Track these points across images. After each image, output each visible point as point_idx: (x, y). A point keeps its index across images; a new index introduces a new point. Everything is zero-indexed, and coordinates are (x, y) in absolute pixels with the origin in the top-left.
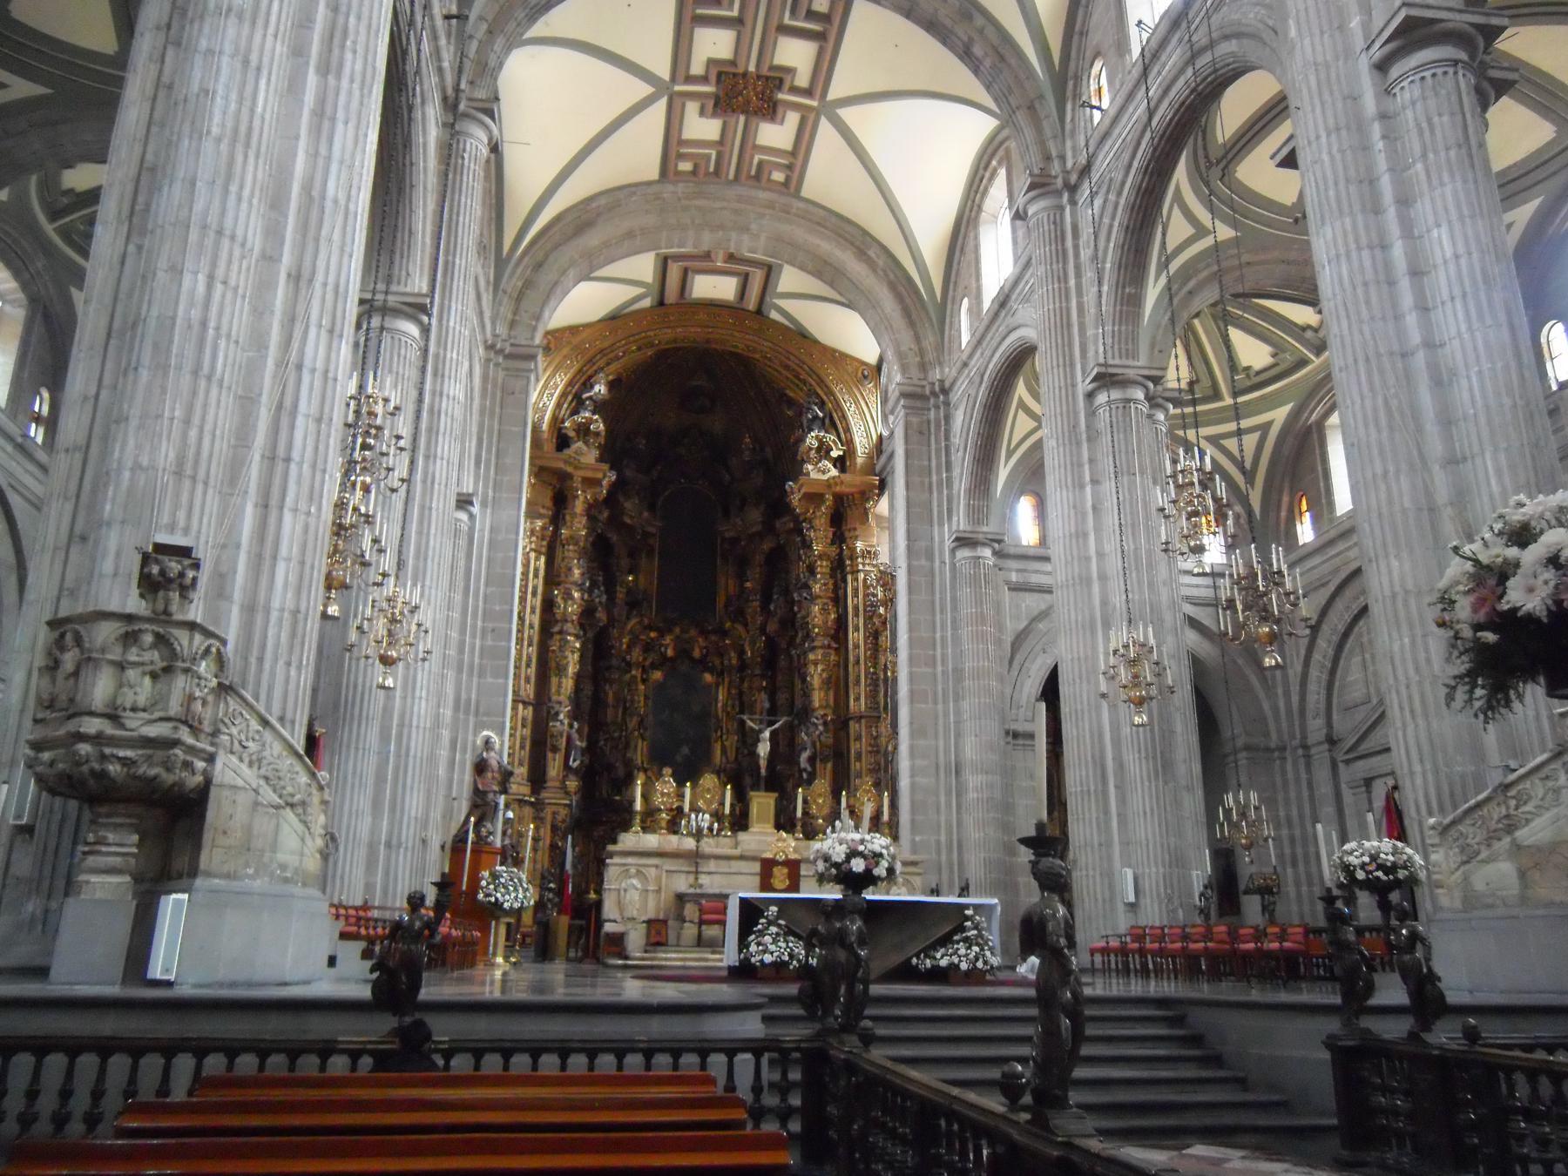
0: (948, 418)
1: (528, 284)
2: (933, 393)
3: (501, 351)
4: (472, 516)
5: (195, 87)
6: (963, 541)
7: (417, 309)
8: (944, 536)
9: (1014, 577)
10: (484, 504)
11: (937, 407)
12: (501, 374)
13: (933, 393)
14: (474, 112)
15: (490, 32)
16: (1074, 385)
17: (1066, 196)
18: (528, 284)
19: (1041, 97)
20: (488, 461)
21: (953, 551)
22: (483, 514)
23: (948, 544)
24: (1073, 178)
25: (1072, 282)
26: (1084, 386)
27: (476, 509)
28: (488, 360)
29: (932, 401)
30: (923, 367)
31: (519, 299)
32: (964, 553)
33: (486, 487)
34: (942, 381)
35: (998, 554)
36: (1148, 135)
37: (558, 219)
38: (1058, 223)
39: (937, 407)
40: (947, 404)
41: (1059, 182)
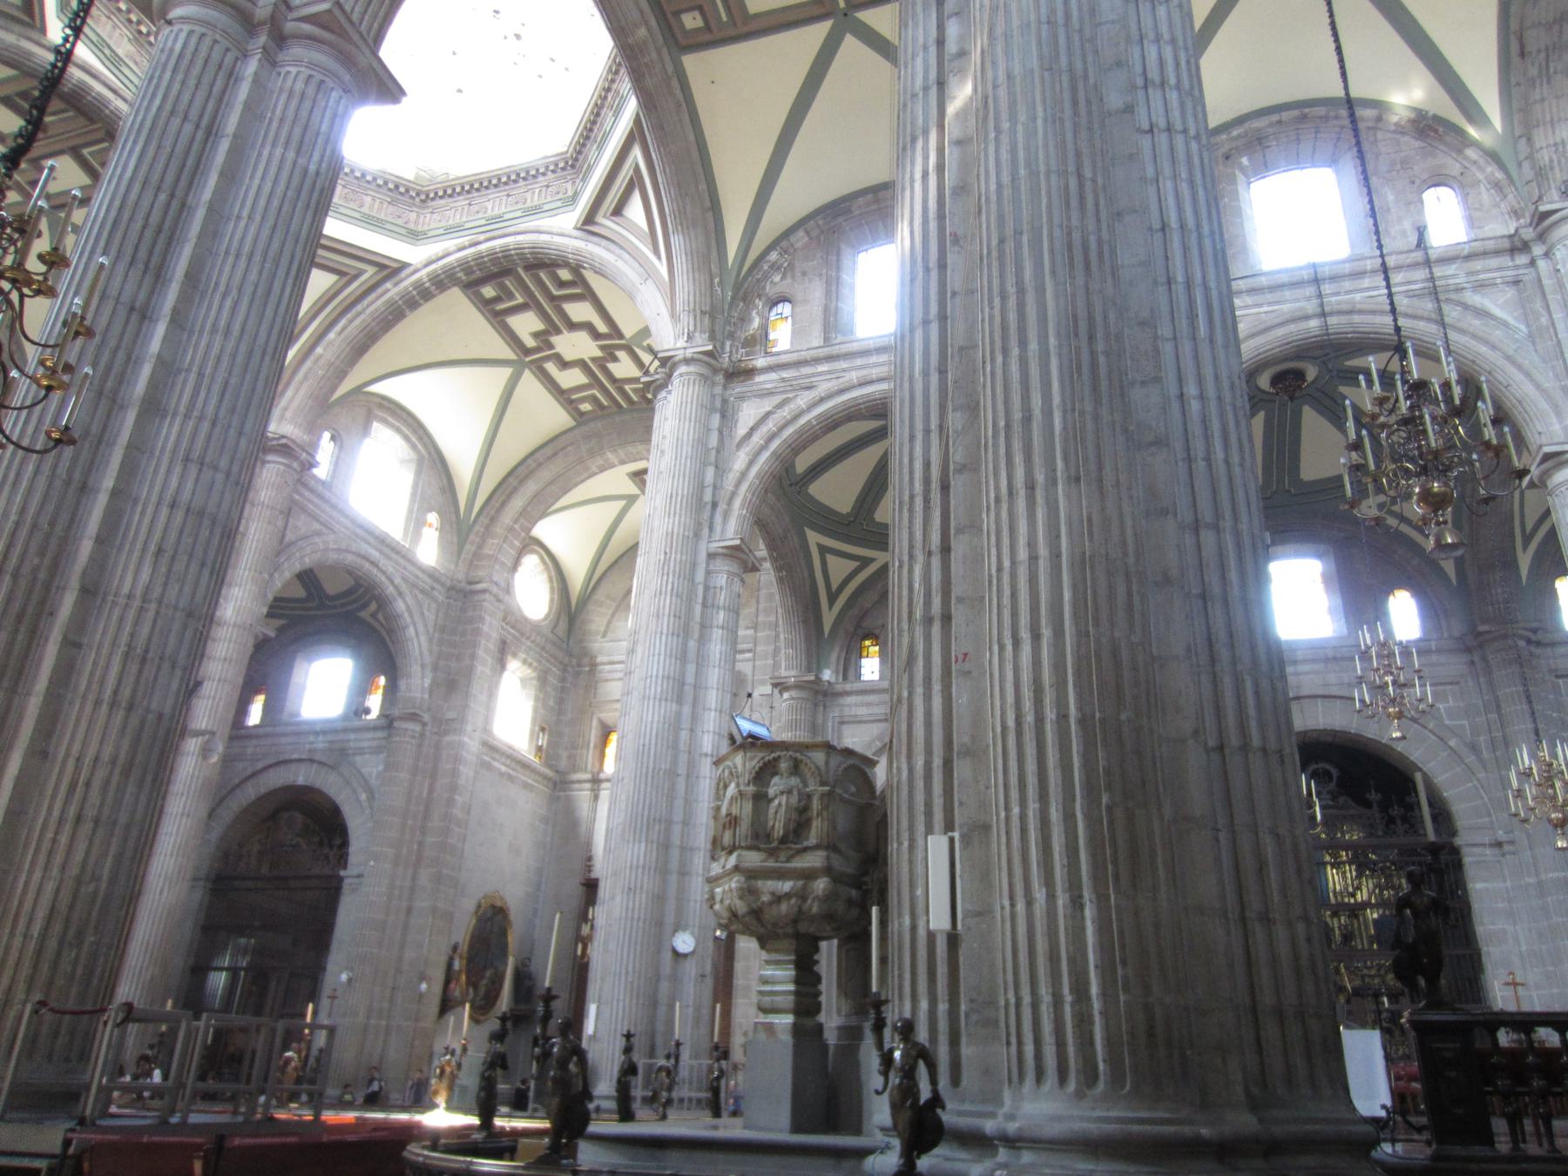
14: (1540, 228)
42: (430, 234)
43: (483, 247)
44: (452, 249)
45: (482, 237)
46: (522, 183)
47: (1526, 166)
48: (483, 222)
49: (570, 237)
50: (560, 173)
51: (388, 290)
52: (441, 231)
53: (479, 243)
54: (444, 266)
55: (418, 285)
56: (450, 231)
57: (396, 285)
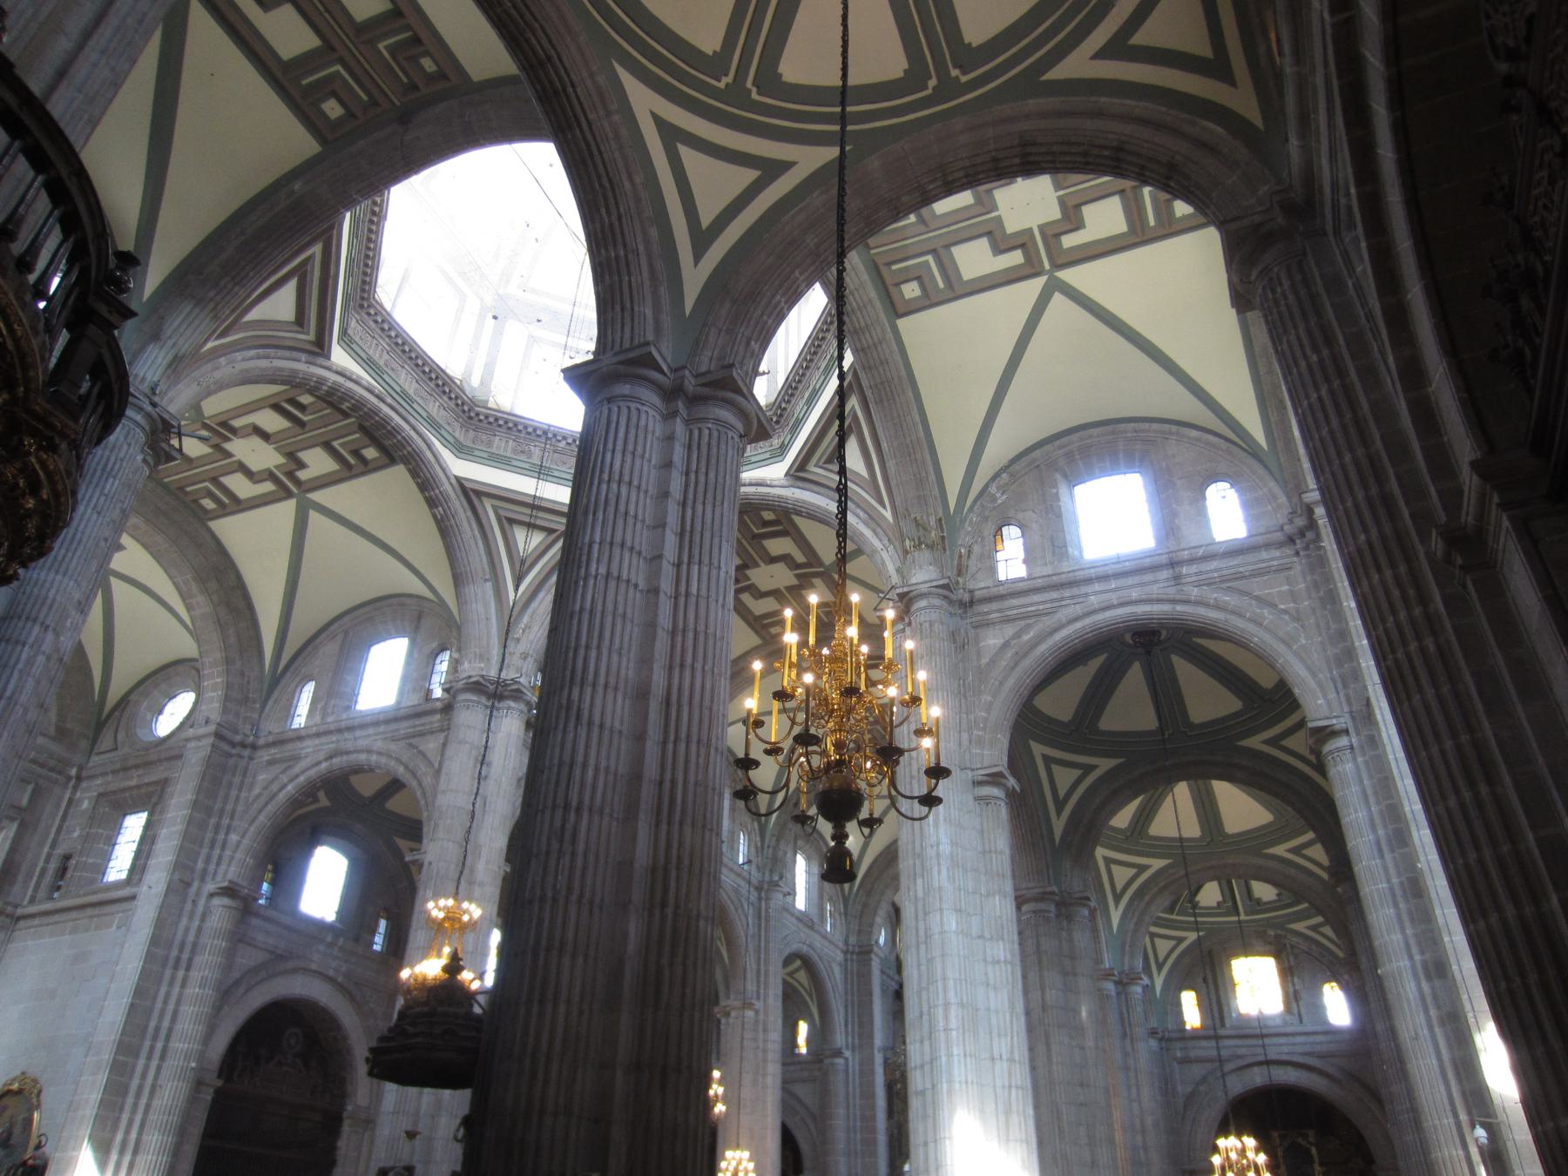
1: (865, 905)
3: (852, 953)
4: (846, 1059)
7: (747, 1005)
9: (1179, 1054)
10: (853, 1051)
12: (855, 965)
15: (778, 840)
18: (865, 905)
20: (853, 1021)
22: (853, 1056)
27: (848, 1054)
28: (846, 960)
31: (861, 917)
33: (853, 1038)
37: (874, 862)
42: (354, 346)
43: (385, 409)
44: (364, 383)
45: (389, 400)
46: (432, 385)
47: (771, 850)
48: (398, 389)
49: (448, 478)
50: (458, 410)
51: (298, 360)
52: (364, 356)
53: (383, 401)
54: (350, 390)
55: (321, 381)
56: (368, 363)
57: (307, 362)
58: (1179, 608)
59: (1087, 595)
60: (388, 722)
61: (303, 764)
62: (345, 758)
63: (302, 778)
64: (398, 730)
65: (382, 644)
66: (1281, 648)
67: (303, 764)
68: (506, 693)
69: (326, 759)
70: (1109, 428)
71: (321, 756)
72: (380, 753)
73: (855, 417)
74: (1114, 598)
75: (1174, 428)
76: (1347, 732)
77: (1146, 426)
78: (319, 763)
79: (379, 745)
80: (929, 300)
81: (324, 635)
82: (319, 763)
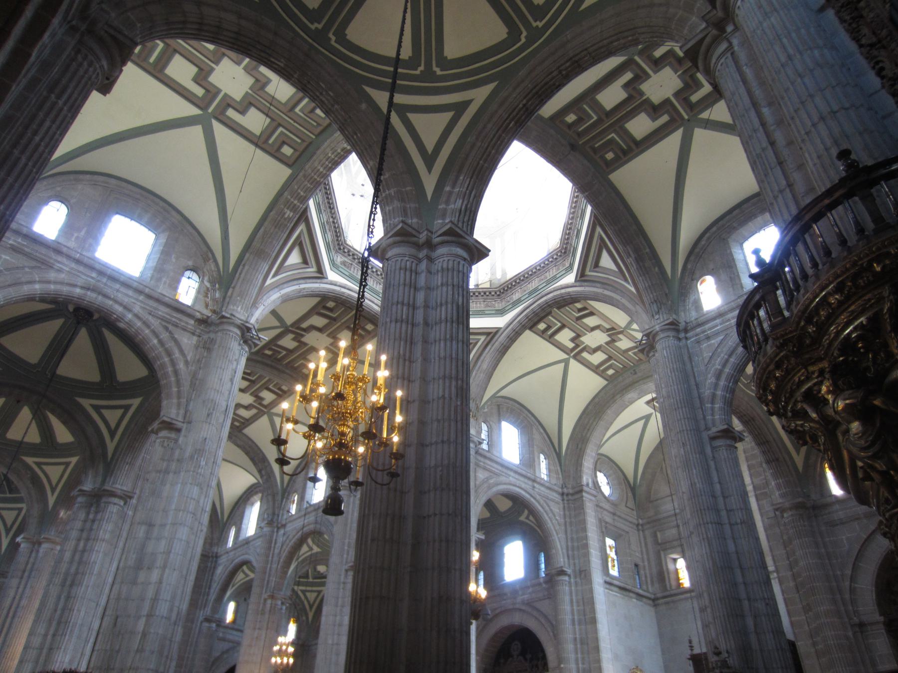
0: (215, 568)
2: (212, 556)
5: (92, 560)
6: (207, 620)
8: (201, 615)
9: (221, 635)
11: (212, 562)
13: (212, 556)
16: (262, 594)
17: (275, 530)
19: (277, 494)
21: (202, 622)
23: (201, 619)
24: (280, 525)
25: (270, 558)
26: (265, 596)
29: (211, 559)
30: (211, 545)
32: (206, 624)
34: (217, 553)
35: (218, 626)
36: (300, 533)
38: (271, 537)
39: (212, 562)
40: (216, 562)
41: (275, 524)
58: (532, 499)
59: (510, 476)
60: (158, 300)
61: (52, 275)
62: (100, 298)
63: (52, 287)
64: (156, 309)
65: (127, 220)
66: (555, 533)
67: (52, 275)
68: (250, 342)
69: (82, 288)
70: (521, 408)
71: (80, 282)
72: (137, 316)
73: (476, 343)
74: (518, 483)
75: (537, 424)
76: (569, 576)
77: (530, 416)
78: (75, 286)
79: (137, 309)
80: (542, 334)
81: (88, 177)
82: (75, 286)
